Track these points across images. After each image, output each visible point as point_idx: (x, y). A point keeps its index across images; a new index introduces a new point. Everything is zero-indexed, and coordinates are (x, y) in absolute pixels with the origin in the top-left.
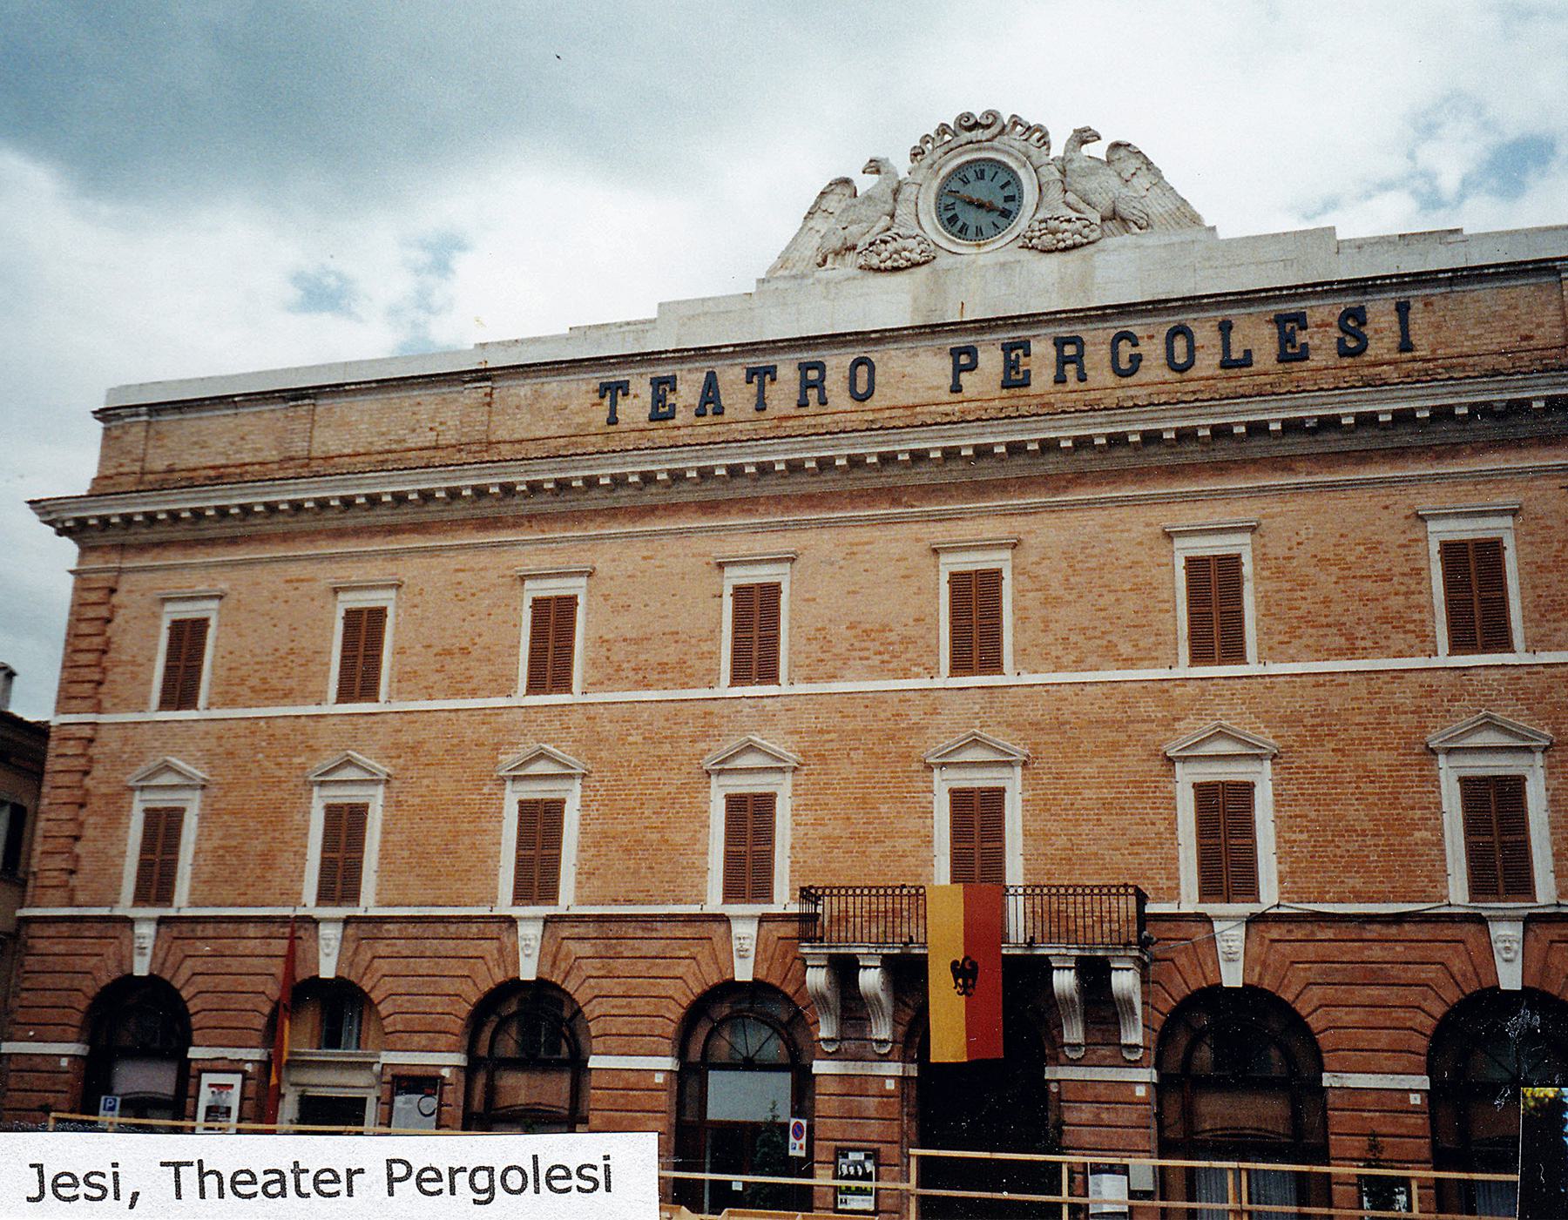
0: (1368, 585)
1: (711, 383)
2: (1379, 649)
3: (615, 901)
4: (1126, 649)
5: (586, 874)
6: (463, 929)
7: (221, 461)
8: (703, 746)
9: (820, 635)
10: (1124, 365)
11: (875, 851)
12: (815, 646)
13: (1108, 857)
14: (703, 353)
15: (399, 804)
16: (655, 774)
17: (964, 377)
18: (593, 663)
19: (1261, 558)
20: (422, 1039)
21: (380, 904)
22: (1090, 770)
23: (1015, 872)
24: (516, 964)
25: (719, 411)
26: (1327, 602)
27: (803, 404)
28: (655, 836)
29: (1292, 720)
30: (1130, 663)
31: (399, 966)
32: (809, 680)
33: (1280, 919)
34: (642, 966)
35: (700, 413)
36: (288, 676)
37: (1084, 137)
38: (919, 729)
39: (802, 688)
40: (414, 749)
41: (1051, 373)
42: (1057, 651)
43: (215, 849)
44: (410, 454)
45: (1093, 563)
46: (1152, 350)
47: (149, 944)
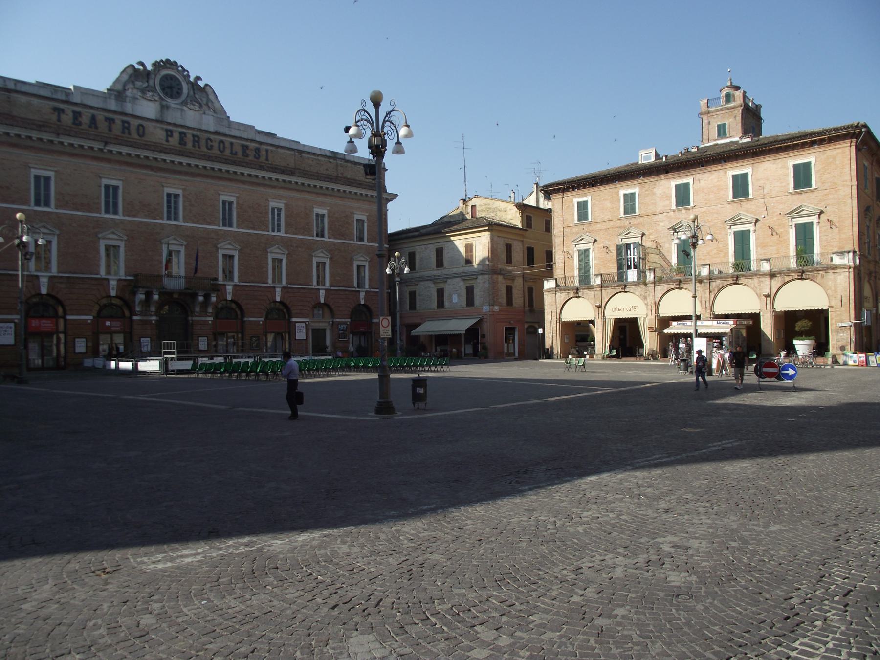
1: (93, 119)
3: (71, 273)
5: (60, 264)
17: (170, 139)
18: (57, 200)
19: (237, 203)
24: (39, 289)
25: (96, 128)
30: (209, 224)
32: (129, 216)
37: (198, 78)
46: (216, 145)
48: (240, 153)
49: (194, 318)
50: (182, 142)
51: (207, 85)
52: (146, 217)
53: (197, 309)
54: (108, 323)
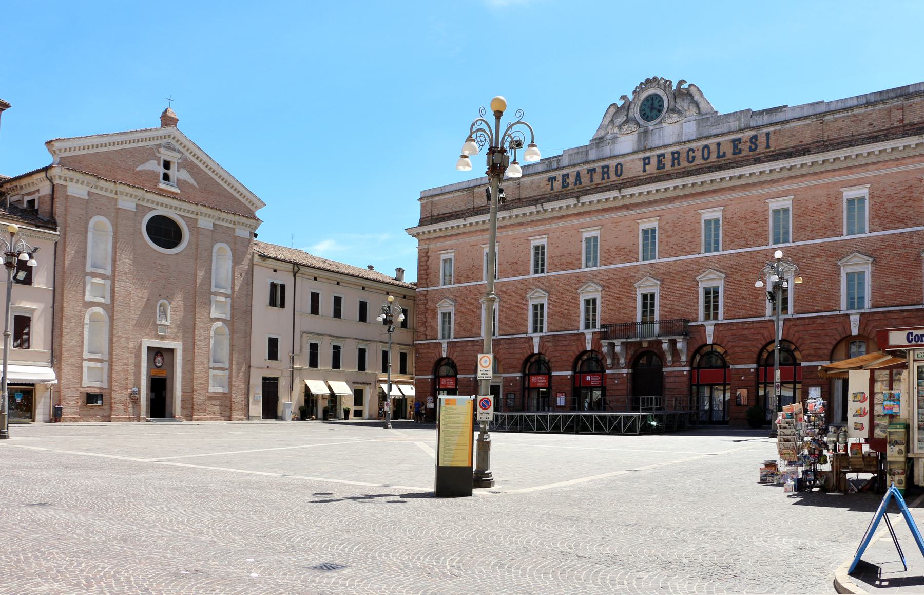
0: (753, 225)
2: (755, 245)
4: (688, 249)
9: (608, 251)
10: (691, 159)
11: (622, 312)
22: (677, 285)
23: (657, 317)
25: (580, 183)
26: (741, 231)
27: (603, 179)
29: (730, 267)
30: (689, 253)
32: (605, 265)
33: (722, 324)
35: (575, 184)
37: (681, 82)
39: (603, 267)
40: (505, 292)
41: (670, 164)
51: (690, 85)
52: (622, 261)
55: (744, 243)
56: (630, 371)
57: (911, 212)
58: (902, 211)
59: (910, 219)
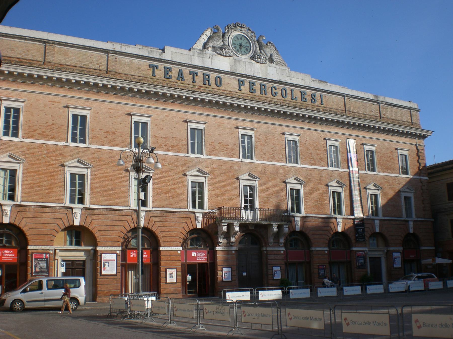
3: (163, 207)
4: (277, 158)
5: (154, 199)
6: (120, 213)
7: (19, 56)
8: (184, 168)
9: (212, 144)
11: (227, 198)
12: (211, 147)
13: (225, 202)
14: (180, 64)
15: (95, 175)
16: (172, 174)
20: (110, 243)
21: (91, 204)
22: (270, 183)
23: (257, 205)
25: (183, 80)
28: (173, 191)
30: (278, 161)
31: (101, 222)
32: (210, 155)
34: (173, 224)
36: (52, 131)
38: (235, 170)
39: (209, 157)
40: (99, 160)
42: (264, 156)
43: (29, 184)
44: (91, 70)
45: (270, 137)
46: (279, 92)
47: (9, 213)
48: (299, 99)
49: (269, 249)
50: (252, 90)
53: (271, 240)
54: (194, 254)
55: (313, 162)
56: (313, 249)
57: (393, 166)
58: (390, 164)
59: (393, 169)
